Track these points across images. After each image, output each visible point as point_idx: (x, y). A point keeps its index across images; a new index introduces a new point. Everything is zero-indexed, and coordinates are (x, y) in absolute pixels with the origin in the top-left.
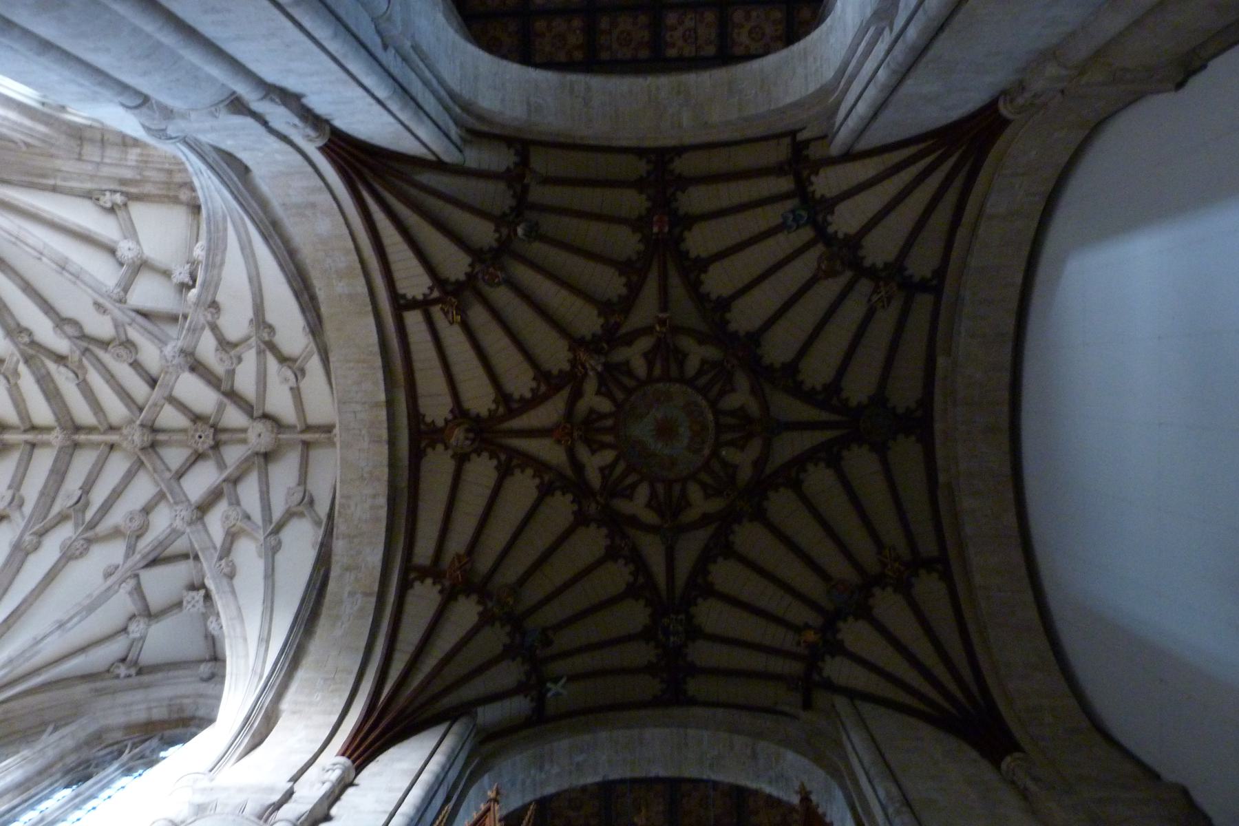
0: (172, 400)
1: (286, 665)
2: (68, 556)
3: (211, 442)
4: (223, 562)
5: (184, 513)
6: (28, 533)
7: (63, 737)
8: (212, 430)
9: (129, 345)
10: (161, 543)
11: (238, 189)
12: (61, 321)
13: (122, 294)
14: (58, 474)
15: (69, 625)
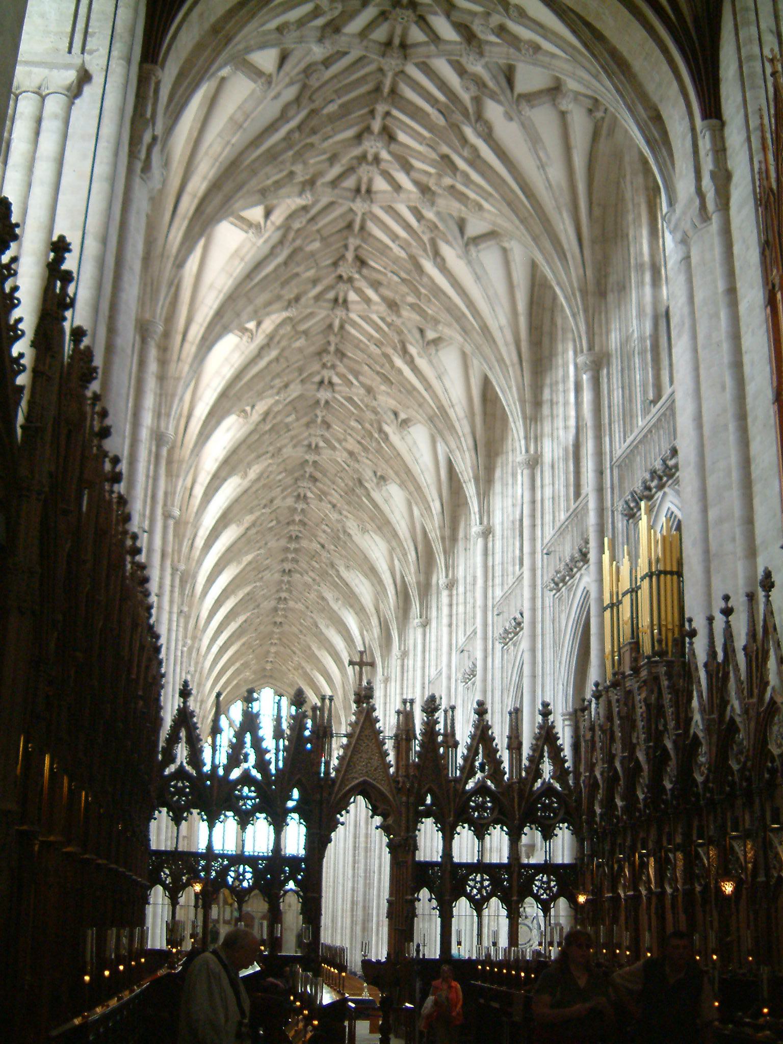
0: (363, 34)
1: (622, 77)
2: (489, 136)
3: (409, 13)
4: (523, 52)
5: (471, 58)
6: (461, 151)
7: (632, 183)
8: (397, 9)
9: (308, 71)
10: (494, 77)
11: (190, 84)
12: (283, 116)
13: (263, 80)
14: (416, 113)
15: (544, 159)
